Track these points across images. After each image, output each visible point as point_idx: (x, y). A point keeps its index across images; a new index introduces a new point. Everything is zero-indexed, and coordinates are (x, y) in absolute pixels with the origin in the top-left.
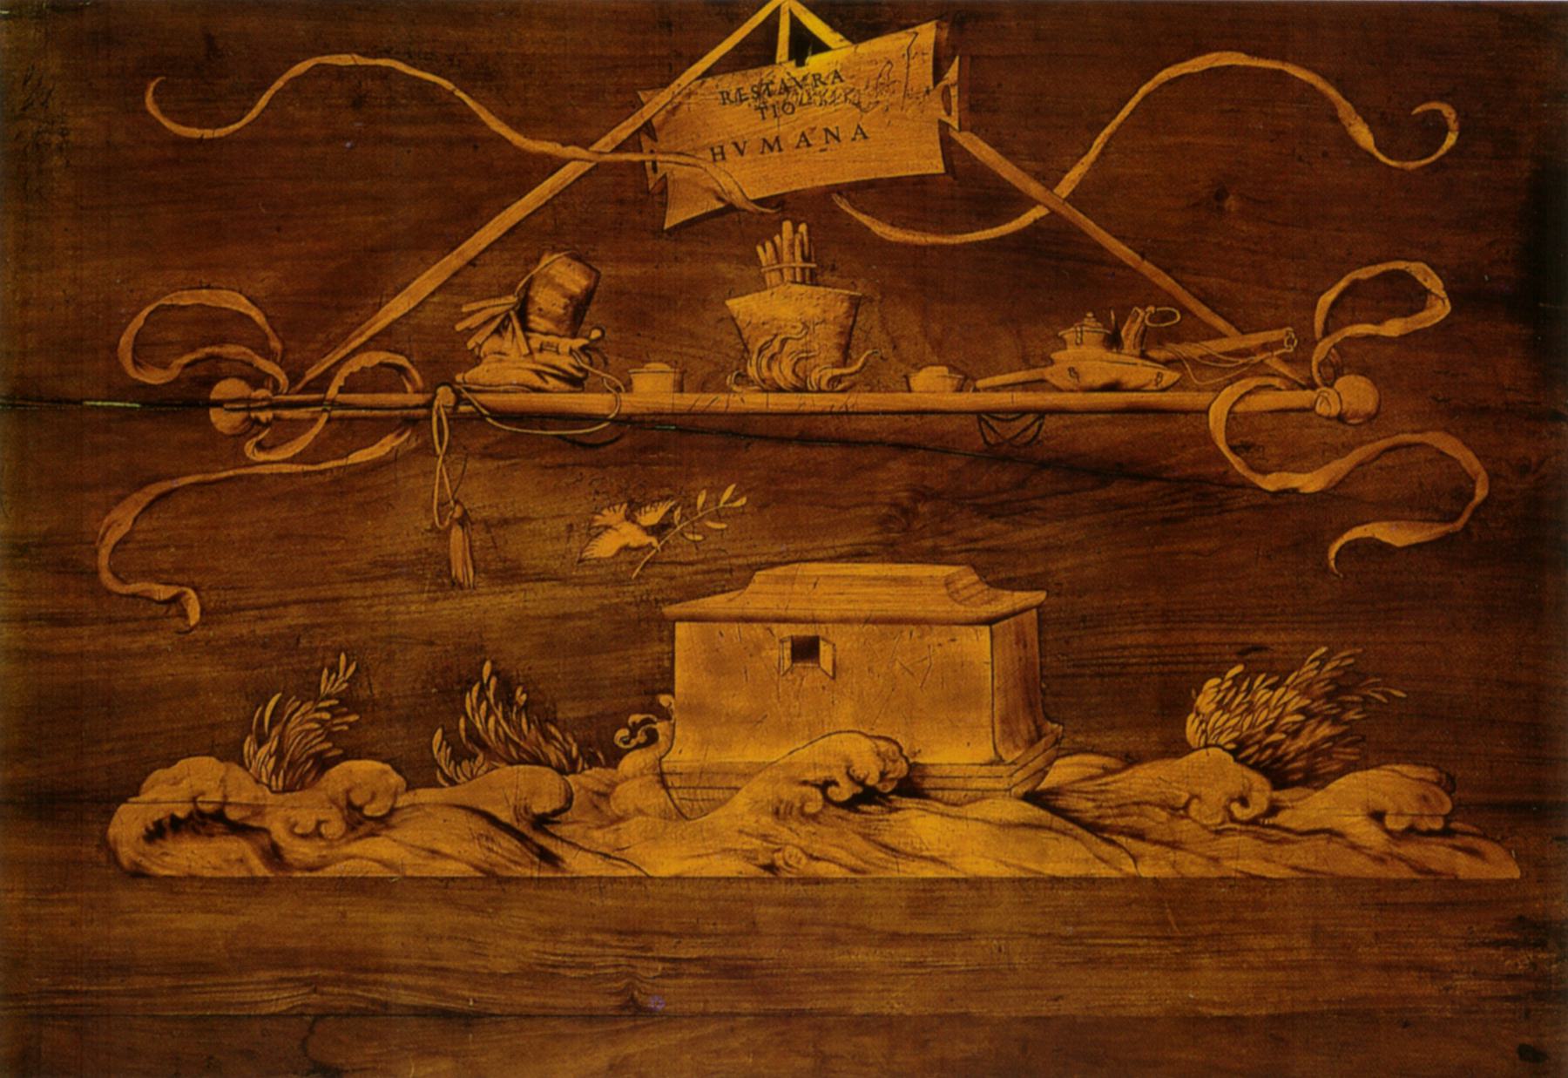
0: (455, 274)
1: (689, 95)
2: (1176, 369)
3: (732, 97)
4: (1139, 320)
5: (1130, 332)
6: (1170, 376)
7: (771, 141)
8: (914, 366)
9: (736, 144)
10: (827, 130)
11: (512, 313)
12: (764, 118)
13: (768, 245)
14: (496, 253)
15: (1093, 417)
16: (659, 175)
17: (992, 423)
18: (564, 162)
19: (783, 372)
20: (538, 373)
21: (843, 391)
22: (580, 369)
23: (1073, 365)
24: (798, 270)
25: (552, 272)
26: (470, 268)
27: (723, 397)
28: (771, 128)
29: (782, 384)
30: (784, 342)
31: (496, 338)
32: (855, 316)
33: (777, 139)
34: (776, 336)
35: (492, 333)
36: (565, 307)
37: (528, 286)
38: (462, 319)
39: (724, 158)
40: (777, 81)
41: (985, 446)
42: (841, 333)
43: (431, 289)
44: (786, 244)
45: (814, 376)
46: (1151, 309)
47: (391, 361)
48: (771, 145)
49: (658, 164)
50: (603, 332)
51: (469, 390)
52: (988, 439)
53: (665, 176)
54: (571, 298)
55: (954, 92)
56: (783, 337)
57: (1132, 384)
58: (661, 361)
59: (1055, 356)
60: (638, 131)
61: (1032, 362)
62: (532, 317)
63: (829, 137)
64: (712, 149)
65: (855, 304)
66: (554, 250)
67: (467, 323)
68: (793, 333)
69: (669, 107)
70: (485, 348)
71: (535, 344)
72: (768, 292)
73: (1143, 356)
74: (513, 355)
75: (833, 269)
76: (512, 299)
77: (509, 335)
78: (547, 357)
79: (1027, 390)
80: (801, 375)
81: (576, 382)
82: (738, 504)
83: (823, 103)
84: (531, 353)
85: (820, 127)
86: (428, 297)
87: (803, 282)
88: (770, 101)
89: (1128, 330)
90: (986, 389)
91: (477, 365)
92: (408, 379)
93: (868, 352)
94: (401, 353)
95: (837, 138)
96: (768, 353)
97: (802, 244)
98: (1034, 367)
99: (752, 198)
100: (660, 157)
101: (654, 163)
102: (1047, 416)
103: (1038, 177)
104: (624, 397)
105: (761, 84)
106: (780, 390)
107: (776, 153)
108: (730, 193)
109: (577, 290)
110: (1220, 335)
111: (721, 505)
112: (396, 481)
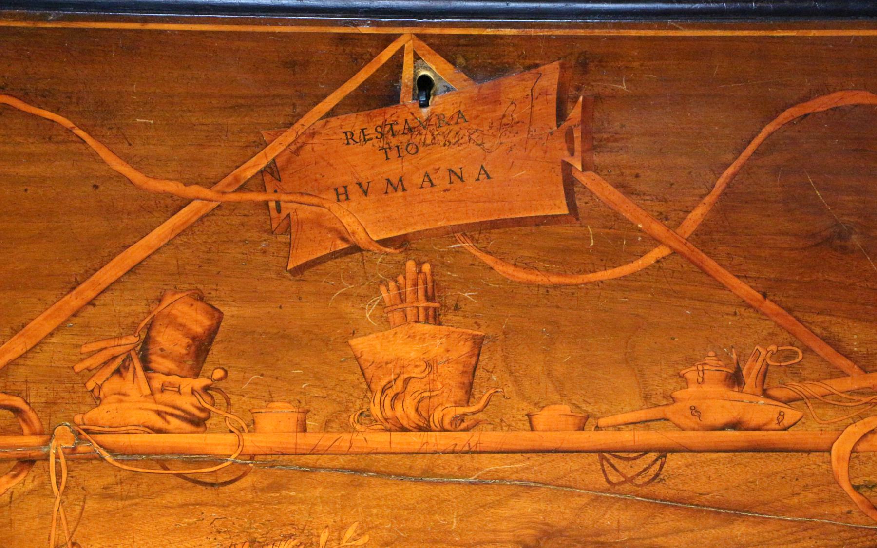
0: (75, 315)
1: (313, 135)
2: (797, 408)
3: (357, 139)
4: (761, 359)
5: (751, 372)
6: (791, 414)
7: (395, 181)
8: (536, 404)
9: (360, 184)
10: (451, 171)
11: (133, 353)
12: (387, 159)
13: (392, 285)
14: (117, 293)
15: (714, 455)
16: (284, 214)
17: (614, 461)
18: (189, 201)
19: (406, 411)
20: (159, 413)
21: (466, 430)
22: (203, 409)
23: (693, 403)
24: (421, 310)
25: (174, 312)
26: (90, 308)
27: (346, 436)
28: (394, 168)
29: (405, 424)
30: (407, 381)
31: (116, 379)
32: (479, 355)
33: (401, 180)
34: (399, 375)
35: (113, 374)
36: (189, 346)
37: (150, 327)
38: (82, 360)
39: (348, 199)
40: (401, 121)
41: (608, 485)
42: (464, 372)
43: (48, 329)
44: (409, 283)
45: (437, 415)
46: (773, 348)
47: (6, 403)
48: (396, 185)
49: (282, 204)
50: (226, 372)
51: (87, 431)
52: (610, 478)
53: (288, 215)
54: (194, 338)
55: (577, 134)
56: (406, 376)
57: (753, 424)
58: (284, 401)
59: (677, 394)
60: (262, 172)
61: (653, 401)
62: (153, 358)
63: (453, 178)
64: (336, 190)
65: (478, 343)
66: (176, 290)
67: (87, 363)
68: (416, 373)
69: (293, 147)
70: (106, 388)
71: (157, 382)
72: (392, 331)
73: (765, 394)
74: (134, 395)
75: (457, 308)
76: (133, 339)
77: (130, 375)
78: (168, 397)
79: (648, 428)
80: (424, 414)
81: (197, 422)
82: (360, 542)
83: (447, 144)
84: (152, 394)
85: (444, 166)
86: (46, 337)
87: (427, 321)
88: (394, 142)
89: (750, 369)
90: (607, 427)
91: (97, 406)
92: (24, 421)
93: (492, 391)
94: (18, 395)
95: (461, 179)
96: (391, 393)
97: (425, 283)
98: (656, 406)
99: (375, 238)
100: (284, 197)
101: (278, 203)
102: (669, 455)
103: (662, 217)
104: (247, 438)
105: (384, 124)
106: (403, 429)
107: (400, 193)
108: (354, 233)
109: (198, 330)
110: (843, 374)
111: (344, 543)
112: (11, 522)
